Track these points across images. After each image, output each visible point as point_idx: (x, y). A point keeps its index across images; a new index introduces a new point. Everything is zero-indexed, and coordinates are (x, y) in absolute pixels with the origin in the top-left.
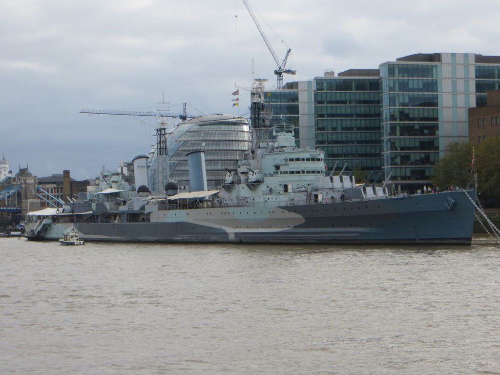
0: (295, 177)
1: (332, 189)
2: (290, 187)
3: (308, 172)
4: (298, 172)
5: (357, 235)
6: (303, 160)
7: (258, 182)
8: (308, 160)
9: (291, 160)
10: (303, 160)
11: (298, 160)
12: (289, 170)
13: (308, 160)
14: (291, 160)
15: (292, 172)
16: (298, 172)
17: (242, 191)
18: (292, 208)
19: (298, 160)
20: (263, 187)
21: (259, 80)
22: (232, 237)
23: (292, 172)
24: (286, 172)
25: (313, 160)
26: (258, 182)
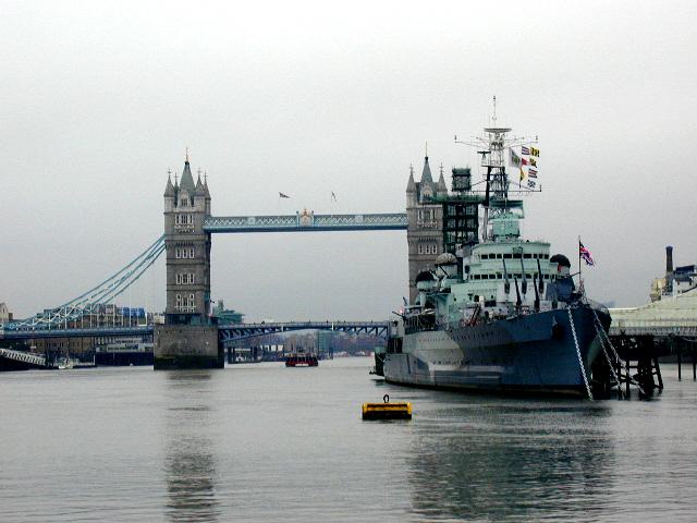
2: (481, 298)
4: (492, 277)
5: (497, 377)
6: (499, 256)
8: (507, 256)
9: (484, 257)
10: (499, 256)
11: (492, 256)
12: (481, 273)
14: (484, 257)
15: (485, 277)
16: (492, 277)
19: (492, 256)
20: (450, 300)
23: (485, 277)
24: (477, 277)
25: (517, 256)
26: (448, 290)
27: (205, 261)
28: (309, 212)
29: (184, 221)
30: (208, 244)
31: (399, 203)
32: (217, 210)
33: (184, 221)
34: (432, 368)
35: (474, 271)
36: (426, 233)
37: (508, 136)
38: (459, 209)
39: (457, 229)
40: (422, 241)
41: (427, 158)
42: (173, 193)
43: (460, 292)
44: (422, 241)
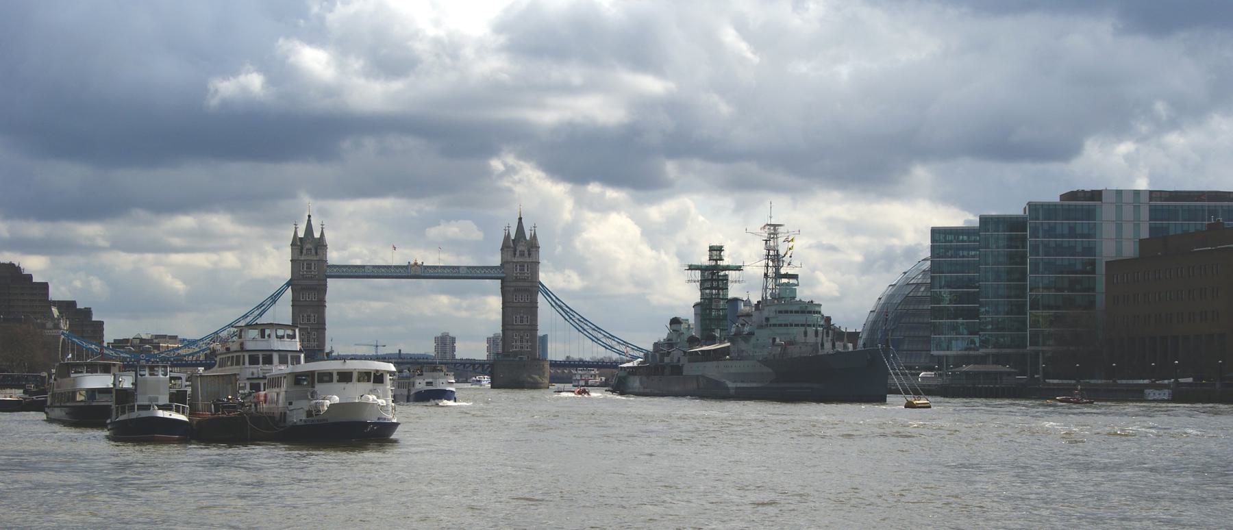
0: (783, 330)
1: (805, 344)
2: (778, 340)
3: (797, 325)
4: (786, 325)
7: (751, 334)
8: (797, 312)
9: (780, 312)
11: (786, 312)
13: (797, 312)
14: (780, 312)
16: (786, 325)
17: (742, 345)
18: (765, 362)
19: (786, 312)
20: (753, 340)
21: (775, 226)
22: (732, 391)
25: (803, 312)
27: (321, 305)
28: (419, 263)
29: (309, 267)
30: (323, 289)
31: (496, 260)
32: (334, 257)
33: (309, 267)
34: (730, 385)
35: (772, 321)
36: (520, 284)
37: (780, 229)
38: (713, 274)
39: (711, 288)
40: (517, 290)
41: (520, 219)
42: (299, 245)
43: (764, 335)
44: (517, 290)
